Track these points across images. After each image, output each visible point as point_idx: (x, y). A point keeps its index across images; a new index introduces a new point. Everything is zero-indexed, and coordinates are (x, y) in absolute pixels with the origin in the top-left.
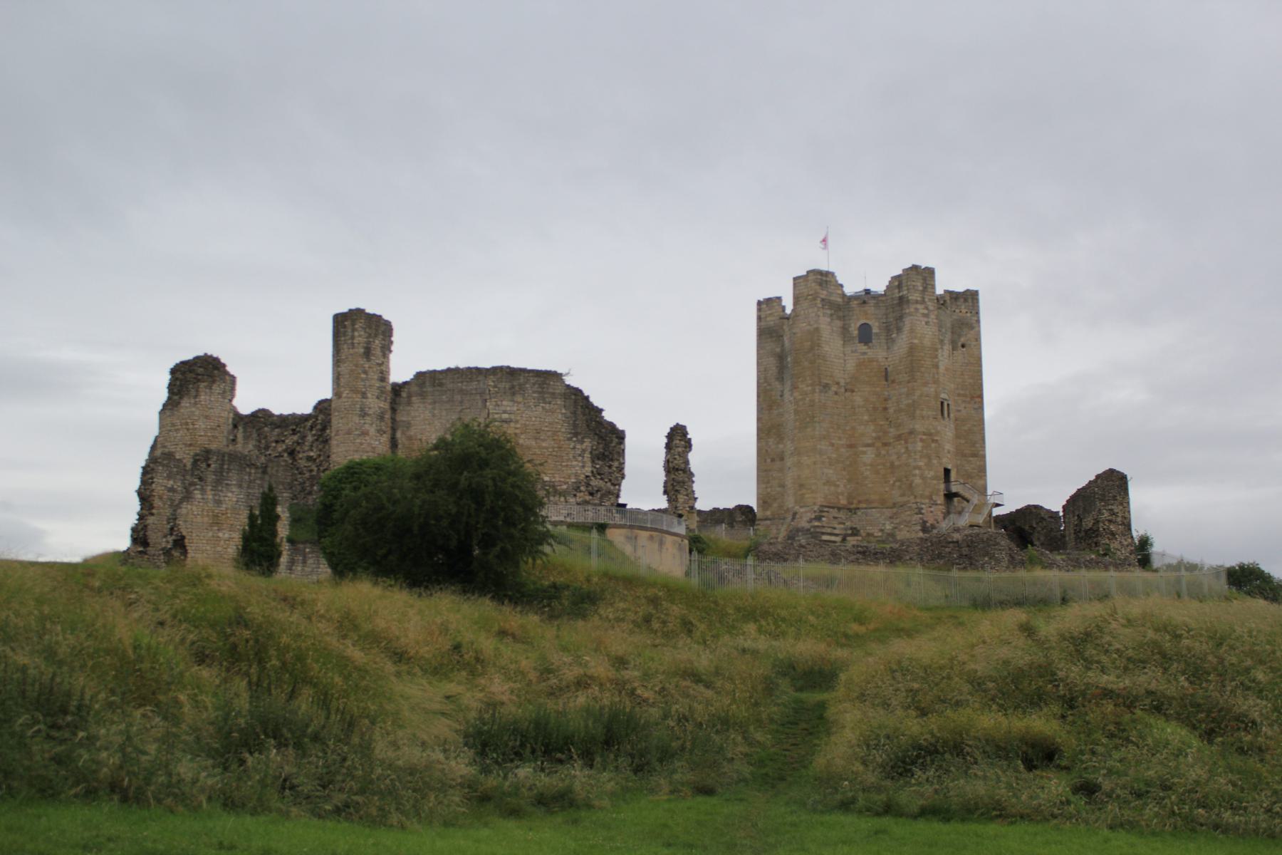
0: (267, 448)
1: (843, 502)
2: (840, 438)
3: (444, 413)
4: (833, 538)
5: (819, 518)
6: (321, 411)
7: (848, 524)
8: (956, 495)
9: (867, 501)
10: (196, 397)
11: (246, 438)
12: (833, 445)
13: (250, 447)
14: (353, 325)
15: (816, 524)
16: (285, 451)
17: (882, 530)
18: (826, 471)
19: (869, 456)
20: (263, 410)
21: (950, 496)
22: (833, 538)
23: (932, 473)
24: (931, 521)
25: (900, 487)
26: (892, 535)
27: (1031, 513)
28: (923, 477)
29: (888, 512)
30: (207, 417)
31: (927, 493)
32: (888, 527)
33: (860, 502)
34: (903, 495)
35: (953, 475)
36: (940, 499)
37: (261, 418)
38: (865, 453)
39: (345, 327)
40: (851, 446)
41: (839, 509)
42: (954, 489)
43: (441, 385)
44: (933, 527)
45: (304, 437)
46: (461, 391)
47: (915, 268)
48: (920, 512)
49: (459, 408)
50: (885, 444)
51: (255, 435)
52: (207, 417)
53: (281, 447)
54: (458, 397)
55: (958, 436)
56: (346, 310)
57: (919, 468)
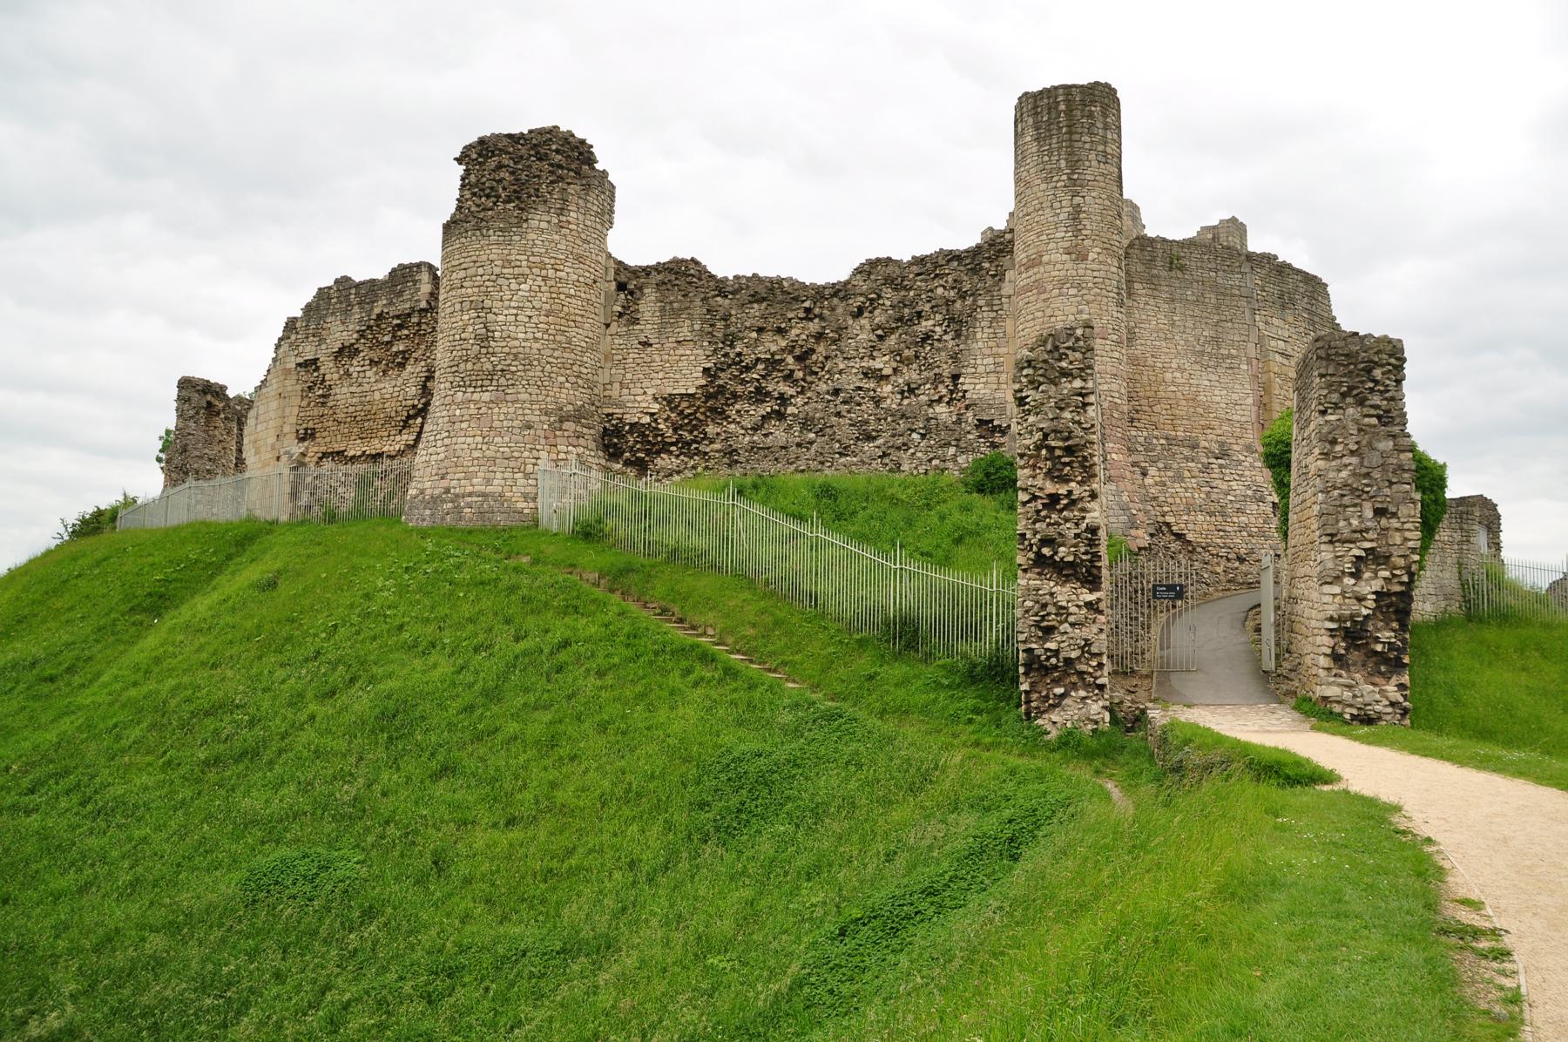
0: (730, 340)
3: (1190, 324)
6: (889, 281)
10: (561, 211)
11: (670, 314)
13: (685, 332)
14: (1105, 116)
16: (791, 349)
20: (693, 260)
30: (579, 258)
37: (681, 277)
39: (1091, 115)
43: (1182, 268)
45: (840, 330)
46: (1215, 287)
47: (1234, 220)
49: (1216, 317)
51: (698, 309)
52: (579, 258)
53: (772, 344)
54: (1211, 298)
56: (1084, 80)
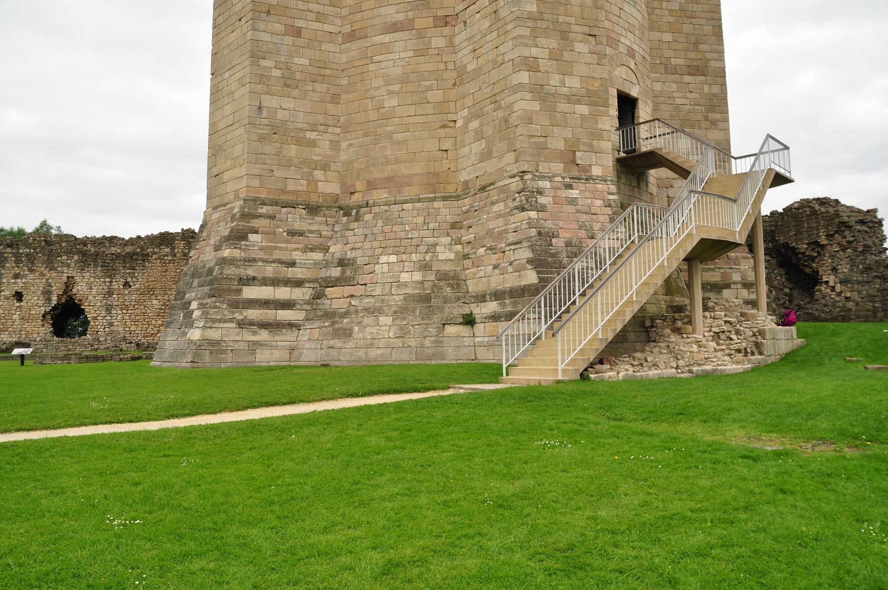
1: (329, 187)
2: (320, 17)
4: (283, 293)
5: (238, 237)
7: (336, 249)
8: (654, 159)
9: (392, 182)
12: (298, 33)
15: (226, 253)
17: (425, 267)
18: (269, 101)
19: (397, 56)
21: (634, 166)
22: (283, 293)
23: (573, 82)
24: (566, 233)
25: (479, 135)
26: (454, 280)
27: (814, 213)
28: (539, 91)
29: (446, 212)
31: (557, 144)
32: (445, 254)
33: (371, 185)
34: (486, 156)
35: (643, 112)
36: (603, 165)
38: (386, 48)
40: (351, 37)
41: (313, 210)
42: (648, 138)
44: (575, 250)
48: (529, 200)
50: (444, 21)
55: (653, 25)
57: (531, 65)
